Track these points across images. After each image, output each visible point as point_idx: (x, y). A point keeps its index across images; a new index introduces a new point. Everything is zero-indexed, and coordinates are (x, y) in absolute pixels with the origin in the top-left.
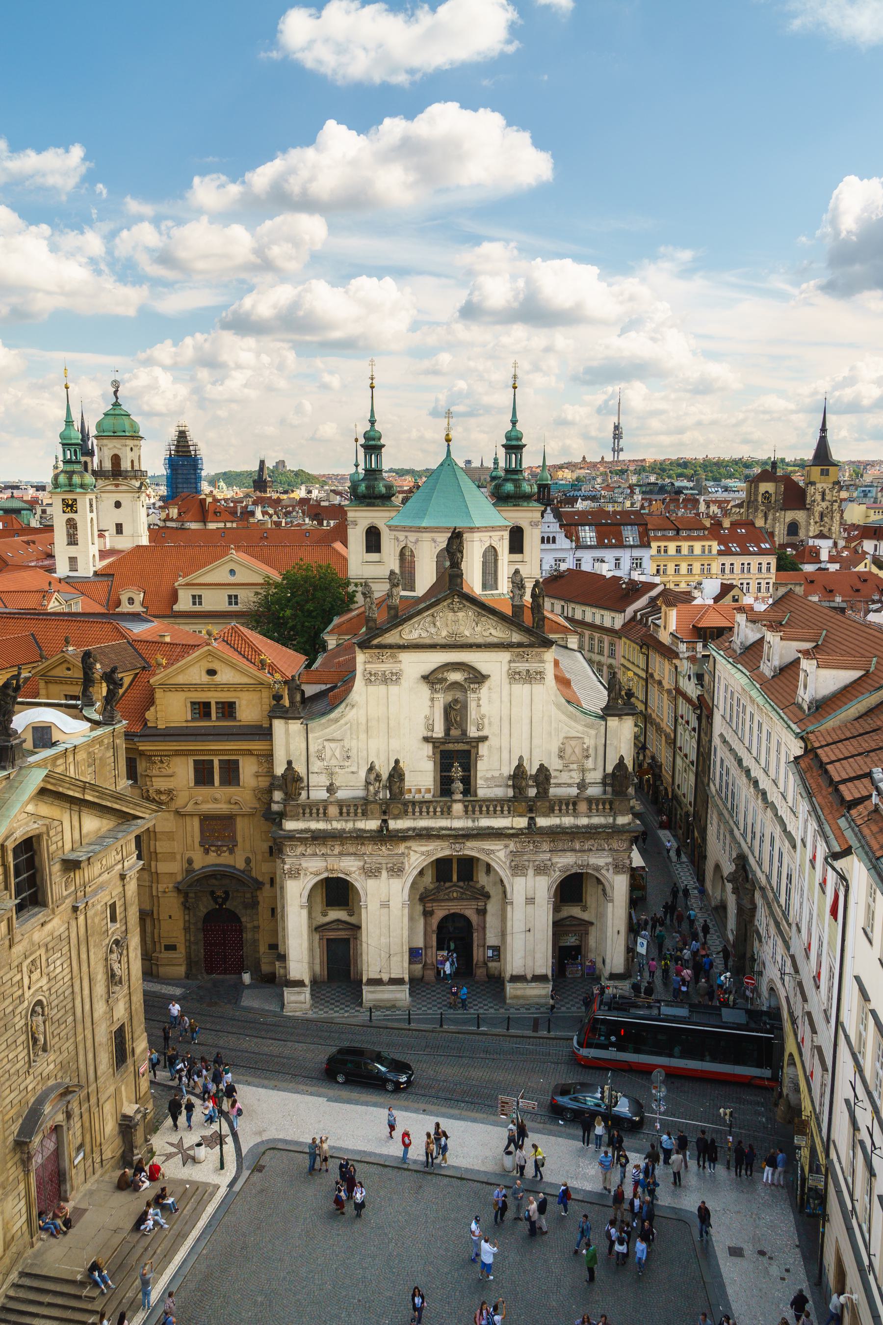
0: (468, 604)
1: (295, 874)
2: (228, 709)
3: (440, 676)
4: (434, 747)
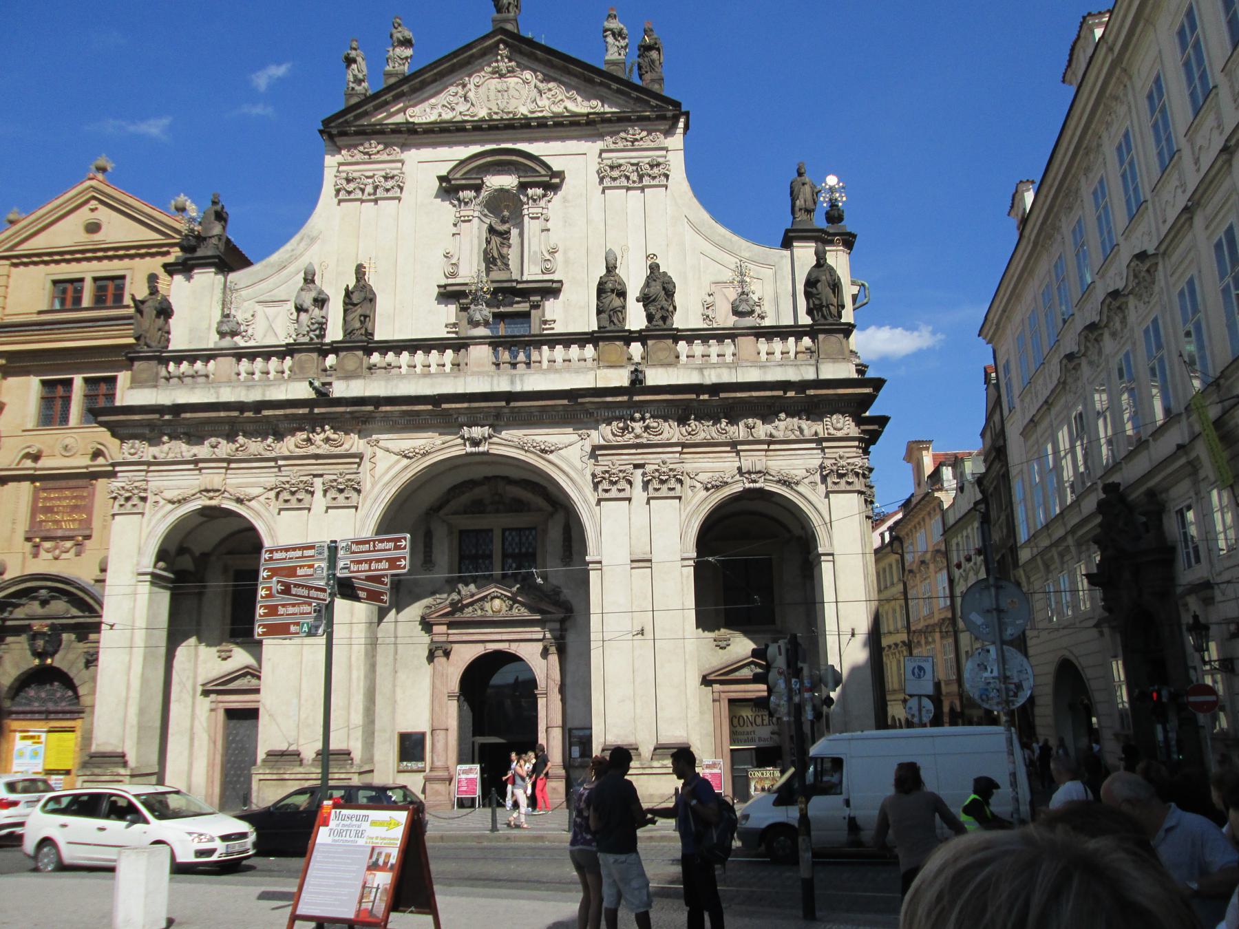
0: (525, 61)
1: (134, 500)
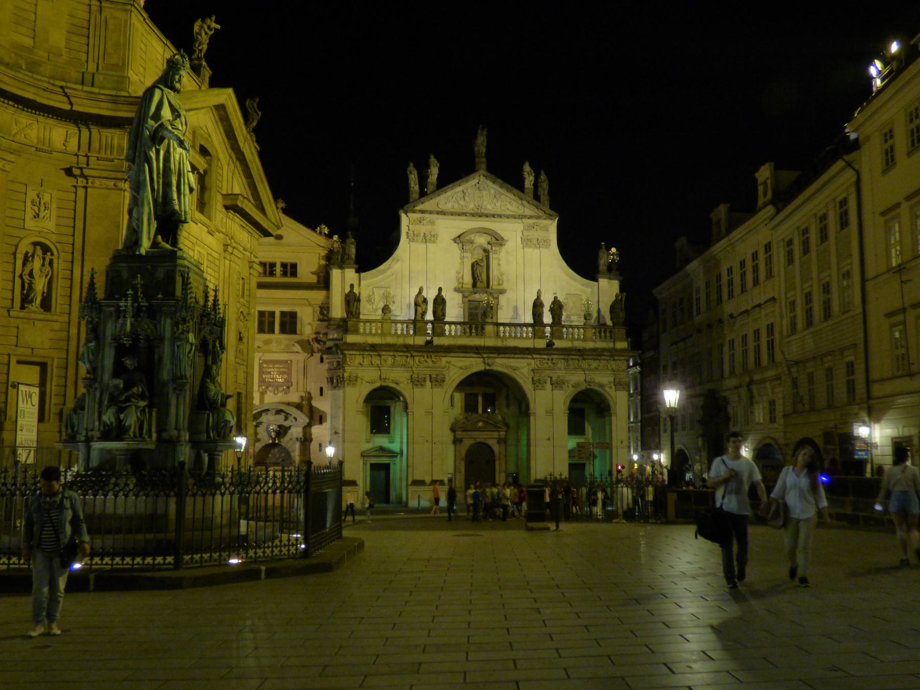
1: (353, 380)
2: (290, 269)
3: (468, 237)
4: (464, 297)
